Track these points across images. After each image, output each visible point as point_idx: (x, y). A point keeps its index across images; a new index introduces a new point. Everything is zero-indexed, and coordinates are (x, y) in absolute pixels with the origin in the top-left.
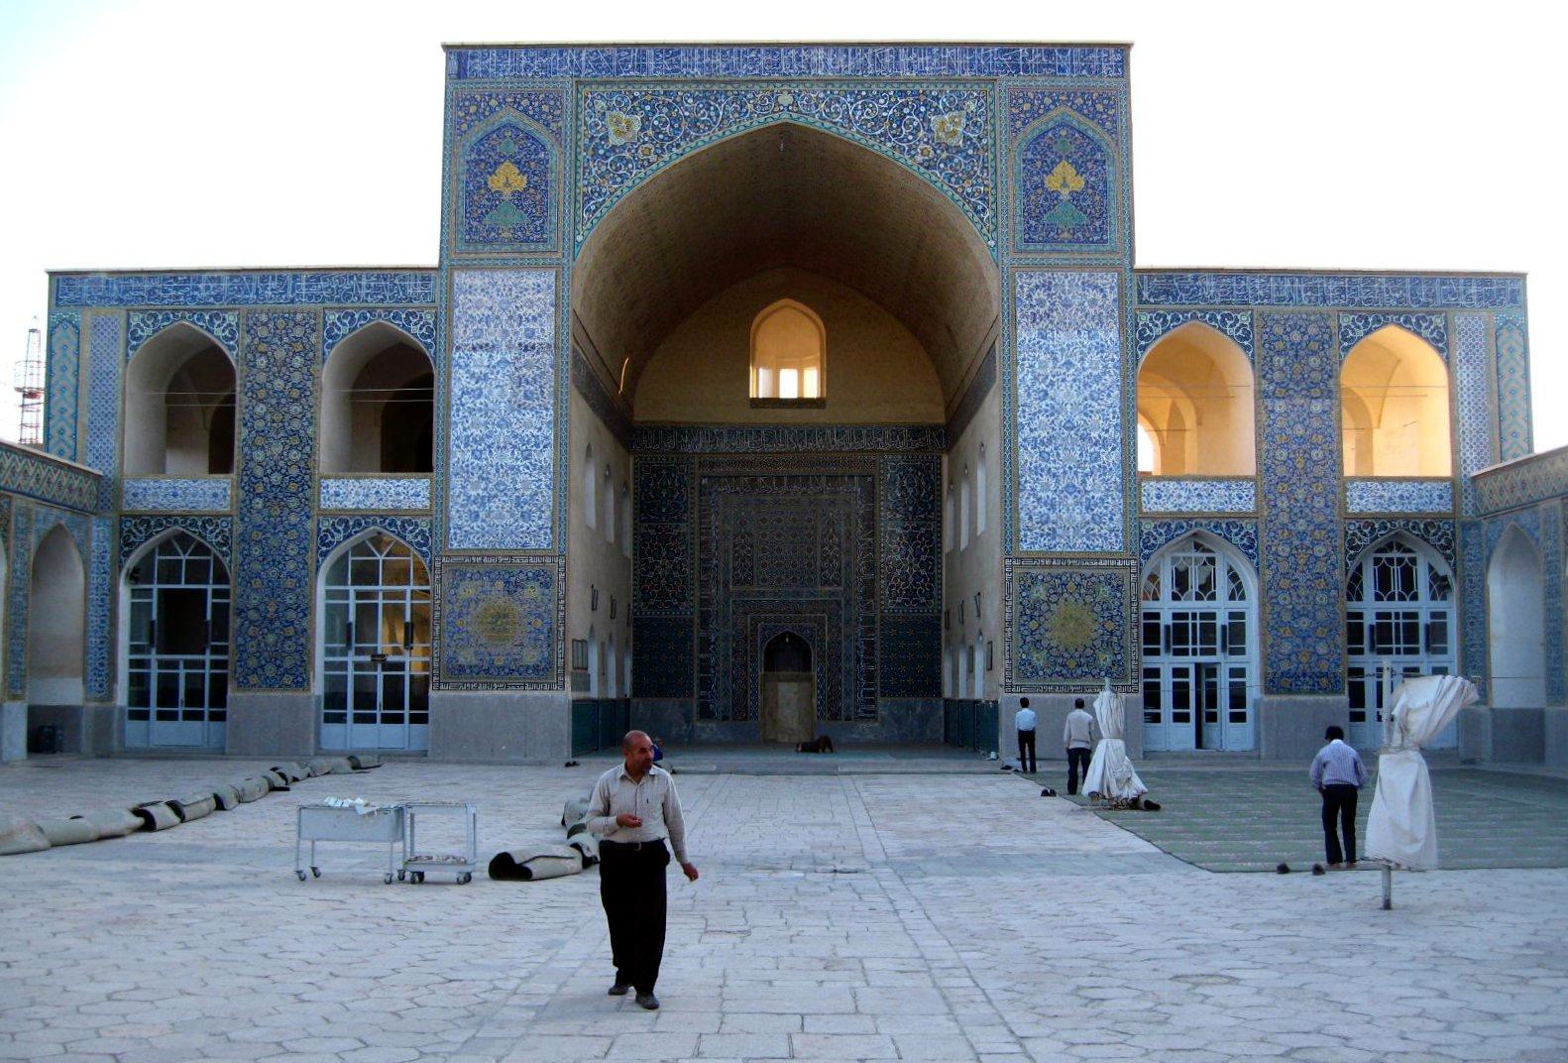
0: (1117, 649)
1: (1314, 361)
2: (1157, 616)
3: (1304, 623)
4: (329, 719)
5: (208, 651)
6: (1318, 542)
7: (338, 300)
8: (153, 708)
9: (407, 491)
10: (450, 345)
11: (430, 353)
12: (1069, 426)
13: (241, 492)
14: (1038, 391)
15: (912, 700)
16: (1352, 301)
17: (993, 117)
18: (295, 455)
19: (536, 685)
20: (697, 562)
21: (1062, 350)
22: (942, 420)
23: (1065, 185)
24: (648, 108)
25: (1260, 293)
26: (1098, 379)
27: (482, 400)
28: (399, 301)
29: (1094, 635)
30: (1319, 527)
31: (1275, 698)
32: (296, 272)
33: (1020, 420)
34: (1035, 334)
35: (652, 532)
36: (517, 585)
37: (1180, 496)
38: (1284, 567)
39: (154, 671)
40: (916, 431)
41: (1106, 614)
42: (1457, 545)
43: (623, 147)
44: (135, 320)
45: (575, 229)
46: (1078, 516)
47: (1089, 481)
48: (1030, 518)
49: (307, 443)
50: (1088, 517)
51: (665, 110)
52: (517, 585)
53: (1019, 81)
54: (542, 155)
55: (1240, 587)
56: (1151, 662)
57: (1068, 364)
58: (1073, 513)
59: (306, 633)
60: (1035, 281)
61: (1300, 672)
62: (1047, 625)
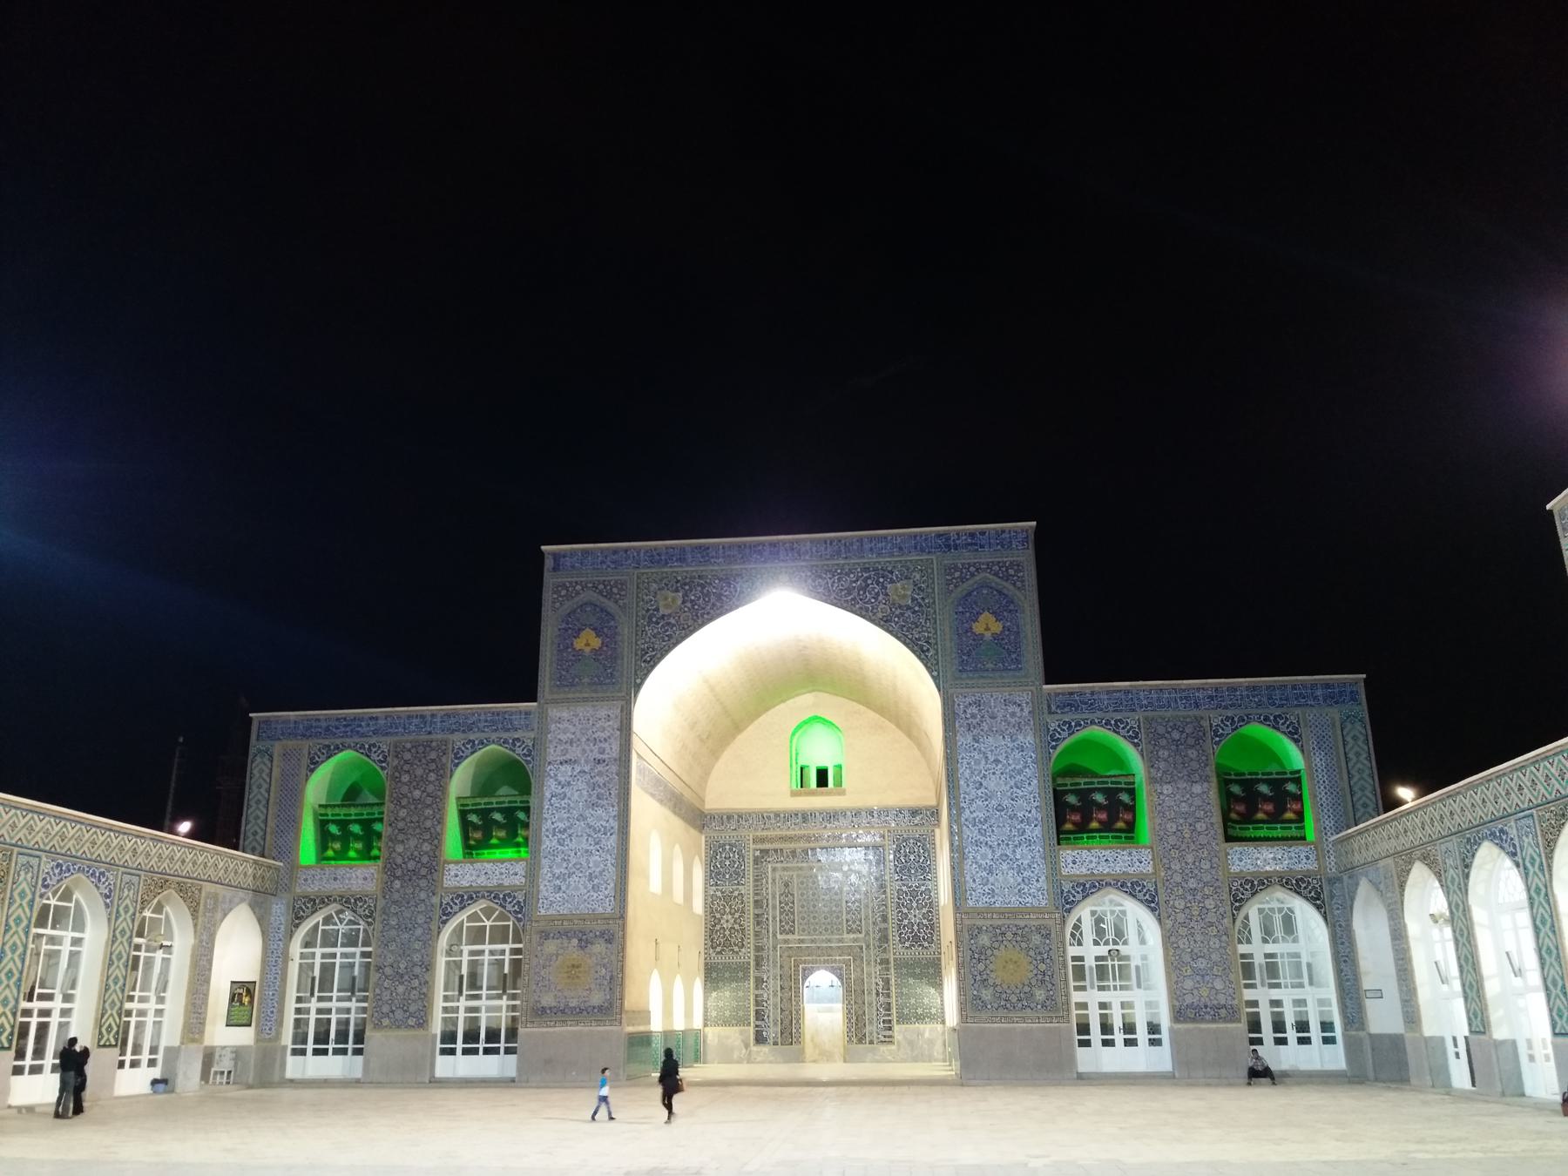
1: (1192, 753)
2: (1081, 959)
3: (1202, 964)
4: (444, 1052)
8: (310, 1046)
11: (529, 768)
12: (1000, 808)
15: (922, 1026)
19: (599, 1022)
23: (987, 629)
26: (1020, 772)
30: (1206, 884)
34: (970, 739)
36: (587, 942)
38: (1181, 917)
39: (313, 1017)
40: (914, 812)
42: (1325, 895)
47: (1018, 851)
52: (587, 942)
60: (968, 700)
62: (991, 967)
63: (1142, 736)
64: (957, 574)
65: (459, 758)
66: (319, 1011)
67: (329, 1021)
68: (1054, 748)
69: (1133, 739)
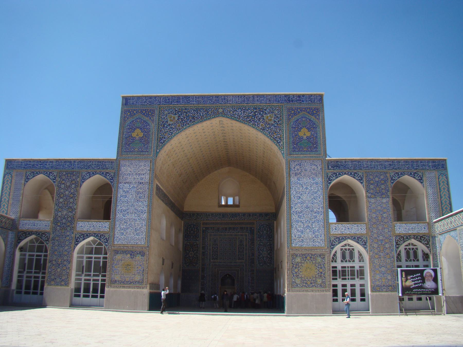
0: (323, 278)
1: (383, 187)
2: (336, 267)
4: (76, 296)
5: (41, 273)
6: (386, 243)
7: (86, 169)
9: (102, 226)
10: (118, 182)
12: (307, 207)
13: (54, 225)
14: (297, 196)
16: (393, 168)
17: (283, 115)
18: (70, 214)
19: (138, 287)
20: (201, 252)
21: (305, 184)
22: (274, 211)
23: (305, 135)
24: (180, 113)
25: (365, 166)
26: (316, 193)
27: (127, 198)
28: (104, 169)
29: (316, 273)
31: (375, 293)
32: (75, 161)
33: (292, 206)
34: (296, 178)
35: (188, 243)
37: (342, 229)
39: (25, 279)
40: (267, 214)
41: (320, 267)
43: (172, 124)
44: (28, 173)
45: (157, 148)
46: (310, 235)
47: (314, 224)
48: (295, 236)
49: (73, 210)
50: (314, 236)
51: (185, 114)
53: (289, 105)
54: (148, 127)
55: (362, 258)
56: (334, 282)
57: (307, 188)
58: (309, 234)
59: (70, 269)
61: (382, 285)
62: (301, 270)
63: (364, 179)
64: (293, 112)
65: (84, 180)
66: (27, 277)
67: (31, 281)
68: (330, 183)
69: (361, 180)
